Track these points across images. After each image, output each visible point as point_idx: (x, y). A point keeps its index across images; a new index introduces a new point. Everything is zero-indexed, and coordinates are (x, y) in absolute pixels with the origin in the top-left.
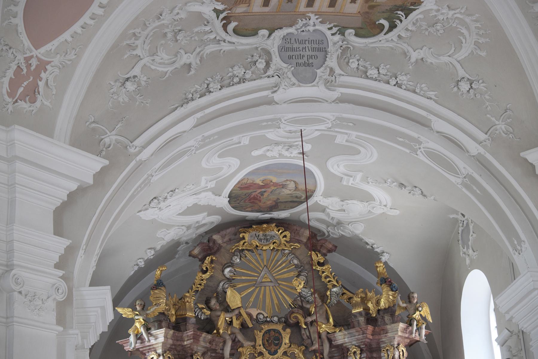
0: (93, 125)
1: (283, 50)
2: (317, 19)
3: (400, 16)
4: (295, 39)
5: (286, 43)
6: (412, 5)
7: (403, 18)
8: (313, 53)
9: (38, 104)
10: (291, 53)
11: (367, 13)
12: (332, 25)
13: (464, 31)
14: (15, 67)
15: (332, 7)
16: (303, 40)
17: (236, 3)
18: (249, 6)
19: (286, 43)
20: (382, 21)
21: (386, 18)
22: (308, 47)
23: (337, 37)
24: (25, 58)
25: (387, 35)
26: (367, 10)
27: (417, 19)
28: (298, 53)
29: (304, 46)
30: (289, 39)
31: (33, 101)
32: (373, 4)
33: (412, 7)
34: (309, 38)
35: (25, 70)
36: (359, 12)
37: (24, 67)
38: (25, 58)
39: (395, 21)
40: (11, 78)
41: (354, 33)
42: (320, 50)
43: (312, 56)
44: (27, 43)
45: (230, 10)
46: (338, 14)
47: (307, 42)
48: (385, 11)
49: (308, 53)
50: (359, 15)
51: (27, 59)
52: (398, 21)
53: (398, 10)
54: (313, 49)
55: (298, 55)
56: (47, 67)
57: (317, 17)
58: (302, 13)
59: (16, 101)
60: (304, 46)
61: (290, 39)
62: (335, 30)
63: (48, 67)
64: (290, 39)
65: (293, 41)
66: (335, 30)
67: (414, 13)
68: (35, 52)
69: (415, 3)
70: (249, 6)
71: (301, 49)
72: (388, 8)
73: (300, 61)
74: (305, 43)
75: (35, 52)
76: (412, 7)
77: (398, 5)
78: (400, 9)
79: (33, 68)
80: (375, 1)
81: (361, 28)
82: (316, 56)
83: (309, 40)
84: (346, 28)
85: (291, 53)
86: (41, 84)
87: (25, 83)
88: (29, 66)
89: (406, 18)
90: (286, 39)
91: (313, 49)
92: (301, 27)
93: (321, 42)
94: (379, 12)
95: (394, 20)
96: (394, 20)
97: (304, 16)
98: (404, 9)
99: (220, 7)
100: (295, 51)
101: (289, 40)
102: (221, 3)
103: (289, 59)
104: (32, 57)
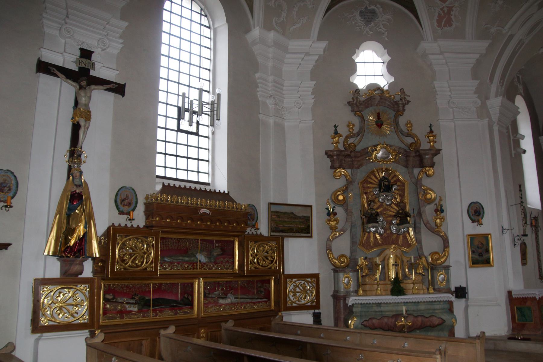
0: (486, 26)
9: (454, 26)
14: (438, 14)
24: (440, 9)
31: (451, 25)
35: (443, 14)
37: (441, 12)
38: (440, 9)
40: (437, 20)
44: (439, 2)
51: (442, 9)
56: (453, 9)
59: (443, 28)
63: (453, 9)
68: (444, 5)
75: (444, 5)
79: (446, 12)
86: (453, 17)
87: (445, 19)
88: (444, 12)
104: (444, 7)
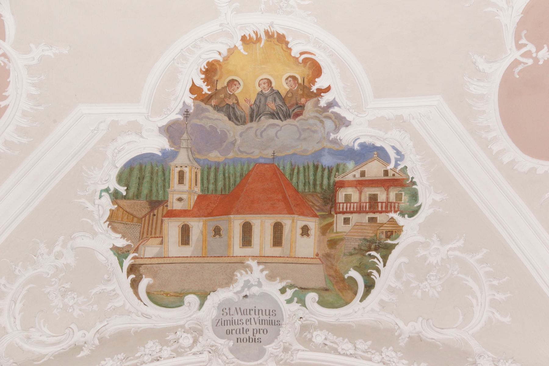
1: (220, 323)
2: (262, 271)
3: (375, 260)
4: (236, 308)
5: (223, 314)
6: (388, 237)
7: (380, 266)
8: (262, 327)
10: (230, 327)
11: (328, 256)
12: (284, 284)
13: (471, 283)
15: (278, 246)
16: (247, 310)
17: (142, 236)
18: (162, 243)
19: (223, 314)
20: (353, 274)
21: (356, 266)
22: (254, 318)
23: (295, 306)
25: (364, 301)
26: (327, 250)
27: (400, 264)
28: (240, 327)
29: (248, 317)
30: (227, 309)
32: (333, 236)
33: (389, 241)
34: (255, 307)
36: (317, 255)
39: (371, 272)
41: (317, 299)
42: (271, 323)
43: (259, 330)
45: (136, 250)
46: (290, 260)
47: (252, 312)
48: (353, 251)
49: (254, 326)
50: (318, 261)
52: (375, 273)
53: (370, 249)
54: (262, 322)
55: (240, 329)
57: (261, 267)
58: (238, 260)
60: (248, 317)
61: (230, 309)
62: (289, 293)
64: (230, 309)
65: (233, 311)
66: (289, 293)
67: (394, 253)
69: (392, 233)
70: (162, 243)
71: (245, 322)
72: (356, 244)
73: (242, 336)
74: (250, 314)
76: (389, 241)
77: (368, 238)
78: (373, 247)
80: (335, 231)
81: (327, 290)
82: (265, 331)
83: (255, 310)
84: (305, 289)
85: (230, 327)
89: (384, 265)
90: (224, 309)
91: (262, 322)
92: (243, 289)
93: (273, 312)
94: (345, 255)
95: (369, 271)
96: (369, 271)
97: (241, 263)
98: (379, 247)
99: (121, 243)
100: (236, 323)
101: (227, 311)
102: (120, 236)
103: (227, 333)
